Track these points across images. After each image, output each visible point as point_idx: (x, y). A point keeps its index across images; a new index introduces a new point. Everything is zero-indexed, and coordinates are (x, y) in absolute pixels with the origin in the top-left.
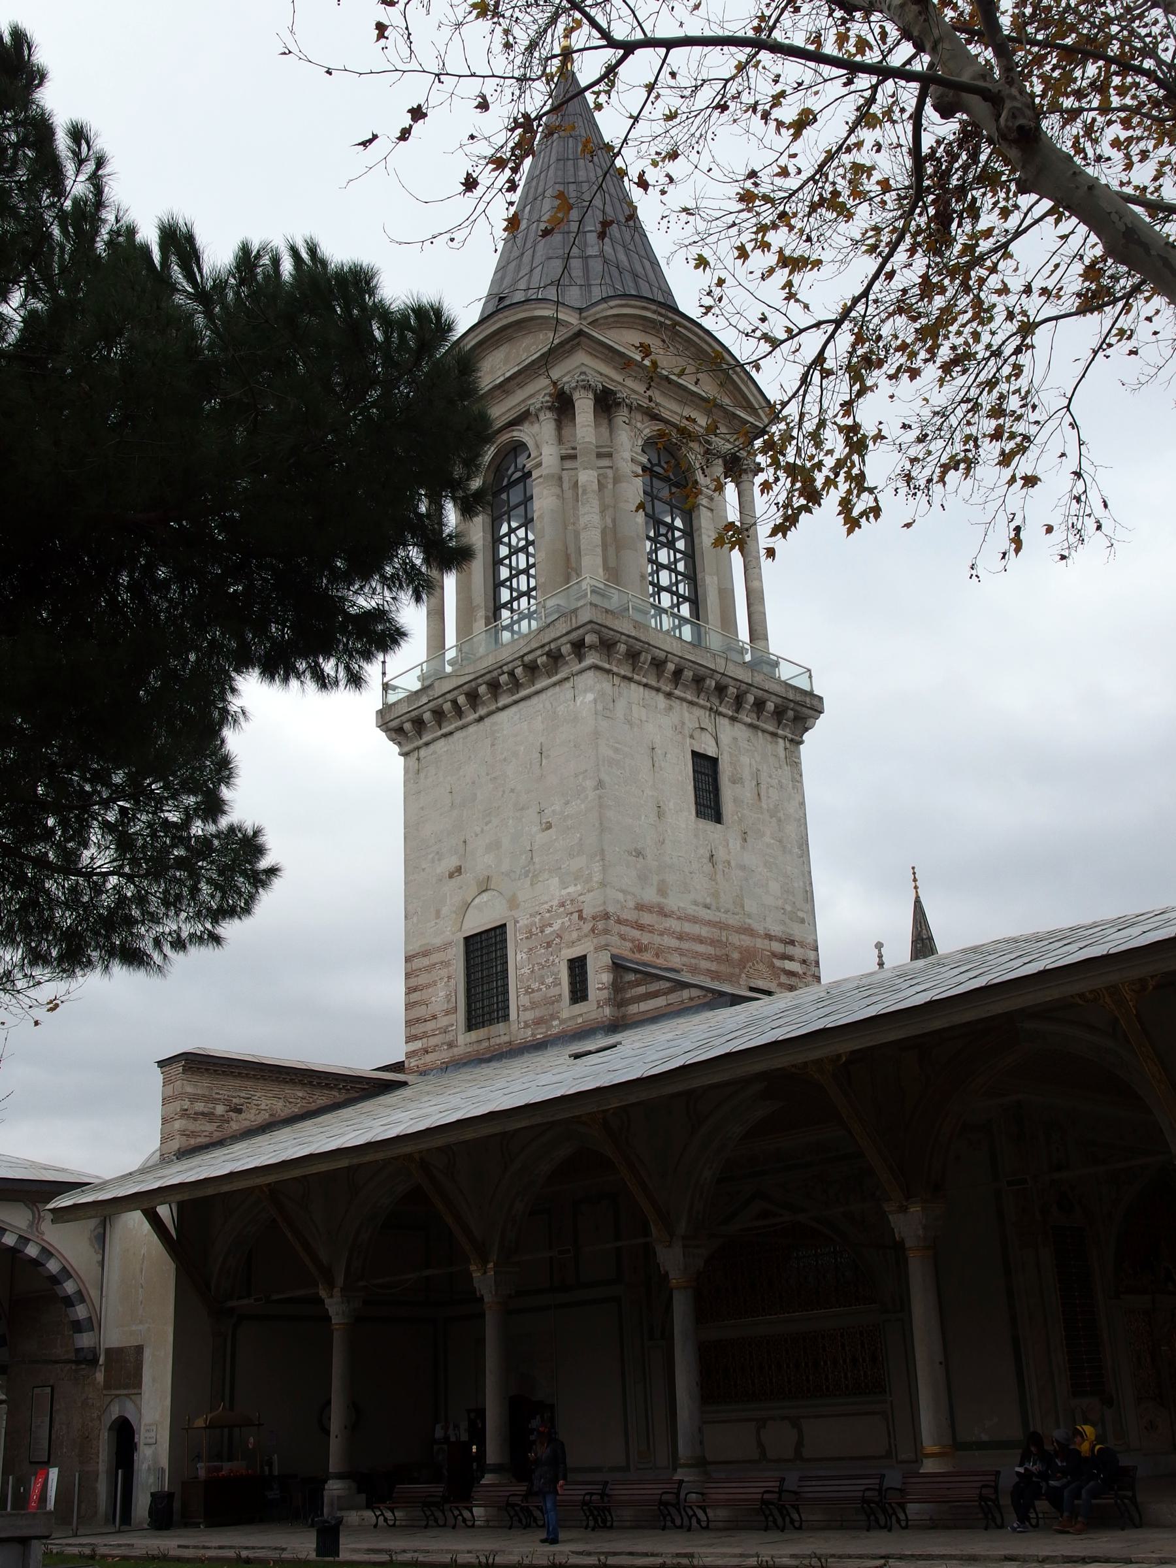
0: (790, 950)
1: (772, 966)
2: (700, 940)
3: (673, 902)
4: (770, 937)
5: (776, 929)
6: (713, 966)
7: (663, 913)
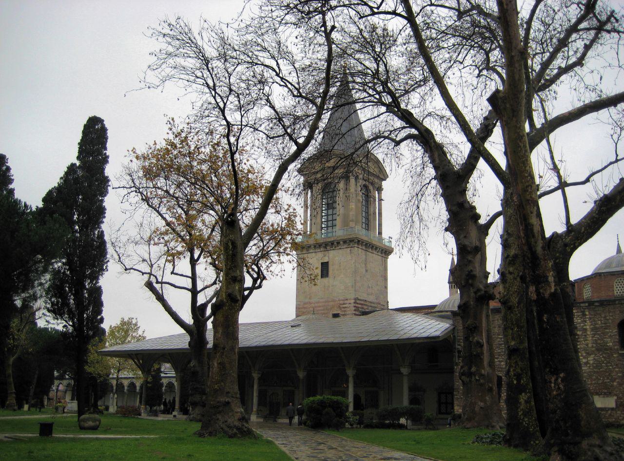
0: (346, 302)
1: (339, 307)
2: (320, 307)
3: (312, 301)
4: (339, 300)
5: (342, 298)
6: (323, 312)
7: (310, 303)
